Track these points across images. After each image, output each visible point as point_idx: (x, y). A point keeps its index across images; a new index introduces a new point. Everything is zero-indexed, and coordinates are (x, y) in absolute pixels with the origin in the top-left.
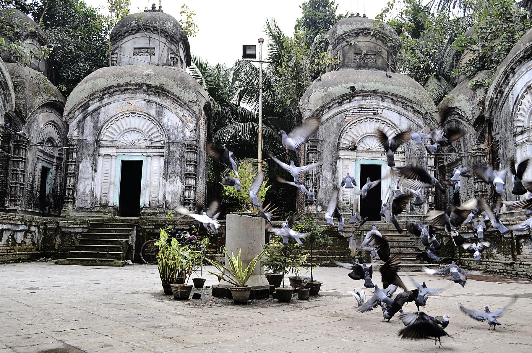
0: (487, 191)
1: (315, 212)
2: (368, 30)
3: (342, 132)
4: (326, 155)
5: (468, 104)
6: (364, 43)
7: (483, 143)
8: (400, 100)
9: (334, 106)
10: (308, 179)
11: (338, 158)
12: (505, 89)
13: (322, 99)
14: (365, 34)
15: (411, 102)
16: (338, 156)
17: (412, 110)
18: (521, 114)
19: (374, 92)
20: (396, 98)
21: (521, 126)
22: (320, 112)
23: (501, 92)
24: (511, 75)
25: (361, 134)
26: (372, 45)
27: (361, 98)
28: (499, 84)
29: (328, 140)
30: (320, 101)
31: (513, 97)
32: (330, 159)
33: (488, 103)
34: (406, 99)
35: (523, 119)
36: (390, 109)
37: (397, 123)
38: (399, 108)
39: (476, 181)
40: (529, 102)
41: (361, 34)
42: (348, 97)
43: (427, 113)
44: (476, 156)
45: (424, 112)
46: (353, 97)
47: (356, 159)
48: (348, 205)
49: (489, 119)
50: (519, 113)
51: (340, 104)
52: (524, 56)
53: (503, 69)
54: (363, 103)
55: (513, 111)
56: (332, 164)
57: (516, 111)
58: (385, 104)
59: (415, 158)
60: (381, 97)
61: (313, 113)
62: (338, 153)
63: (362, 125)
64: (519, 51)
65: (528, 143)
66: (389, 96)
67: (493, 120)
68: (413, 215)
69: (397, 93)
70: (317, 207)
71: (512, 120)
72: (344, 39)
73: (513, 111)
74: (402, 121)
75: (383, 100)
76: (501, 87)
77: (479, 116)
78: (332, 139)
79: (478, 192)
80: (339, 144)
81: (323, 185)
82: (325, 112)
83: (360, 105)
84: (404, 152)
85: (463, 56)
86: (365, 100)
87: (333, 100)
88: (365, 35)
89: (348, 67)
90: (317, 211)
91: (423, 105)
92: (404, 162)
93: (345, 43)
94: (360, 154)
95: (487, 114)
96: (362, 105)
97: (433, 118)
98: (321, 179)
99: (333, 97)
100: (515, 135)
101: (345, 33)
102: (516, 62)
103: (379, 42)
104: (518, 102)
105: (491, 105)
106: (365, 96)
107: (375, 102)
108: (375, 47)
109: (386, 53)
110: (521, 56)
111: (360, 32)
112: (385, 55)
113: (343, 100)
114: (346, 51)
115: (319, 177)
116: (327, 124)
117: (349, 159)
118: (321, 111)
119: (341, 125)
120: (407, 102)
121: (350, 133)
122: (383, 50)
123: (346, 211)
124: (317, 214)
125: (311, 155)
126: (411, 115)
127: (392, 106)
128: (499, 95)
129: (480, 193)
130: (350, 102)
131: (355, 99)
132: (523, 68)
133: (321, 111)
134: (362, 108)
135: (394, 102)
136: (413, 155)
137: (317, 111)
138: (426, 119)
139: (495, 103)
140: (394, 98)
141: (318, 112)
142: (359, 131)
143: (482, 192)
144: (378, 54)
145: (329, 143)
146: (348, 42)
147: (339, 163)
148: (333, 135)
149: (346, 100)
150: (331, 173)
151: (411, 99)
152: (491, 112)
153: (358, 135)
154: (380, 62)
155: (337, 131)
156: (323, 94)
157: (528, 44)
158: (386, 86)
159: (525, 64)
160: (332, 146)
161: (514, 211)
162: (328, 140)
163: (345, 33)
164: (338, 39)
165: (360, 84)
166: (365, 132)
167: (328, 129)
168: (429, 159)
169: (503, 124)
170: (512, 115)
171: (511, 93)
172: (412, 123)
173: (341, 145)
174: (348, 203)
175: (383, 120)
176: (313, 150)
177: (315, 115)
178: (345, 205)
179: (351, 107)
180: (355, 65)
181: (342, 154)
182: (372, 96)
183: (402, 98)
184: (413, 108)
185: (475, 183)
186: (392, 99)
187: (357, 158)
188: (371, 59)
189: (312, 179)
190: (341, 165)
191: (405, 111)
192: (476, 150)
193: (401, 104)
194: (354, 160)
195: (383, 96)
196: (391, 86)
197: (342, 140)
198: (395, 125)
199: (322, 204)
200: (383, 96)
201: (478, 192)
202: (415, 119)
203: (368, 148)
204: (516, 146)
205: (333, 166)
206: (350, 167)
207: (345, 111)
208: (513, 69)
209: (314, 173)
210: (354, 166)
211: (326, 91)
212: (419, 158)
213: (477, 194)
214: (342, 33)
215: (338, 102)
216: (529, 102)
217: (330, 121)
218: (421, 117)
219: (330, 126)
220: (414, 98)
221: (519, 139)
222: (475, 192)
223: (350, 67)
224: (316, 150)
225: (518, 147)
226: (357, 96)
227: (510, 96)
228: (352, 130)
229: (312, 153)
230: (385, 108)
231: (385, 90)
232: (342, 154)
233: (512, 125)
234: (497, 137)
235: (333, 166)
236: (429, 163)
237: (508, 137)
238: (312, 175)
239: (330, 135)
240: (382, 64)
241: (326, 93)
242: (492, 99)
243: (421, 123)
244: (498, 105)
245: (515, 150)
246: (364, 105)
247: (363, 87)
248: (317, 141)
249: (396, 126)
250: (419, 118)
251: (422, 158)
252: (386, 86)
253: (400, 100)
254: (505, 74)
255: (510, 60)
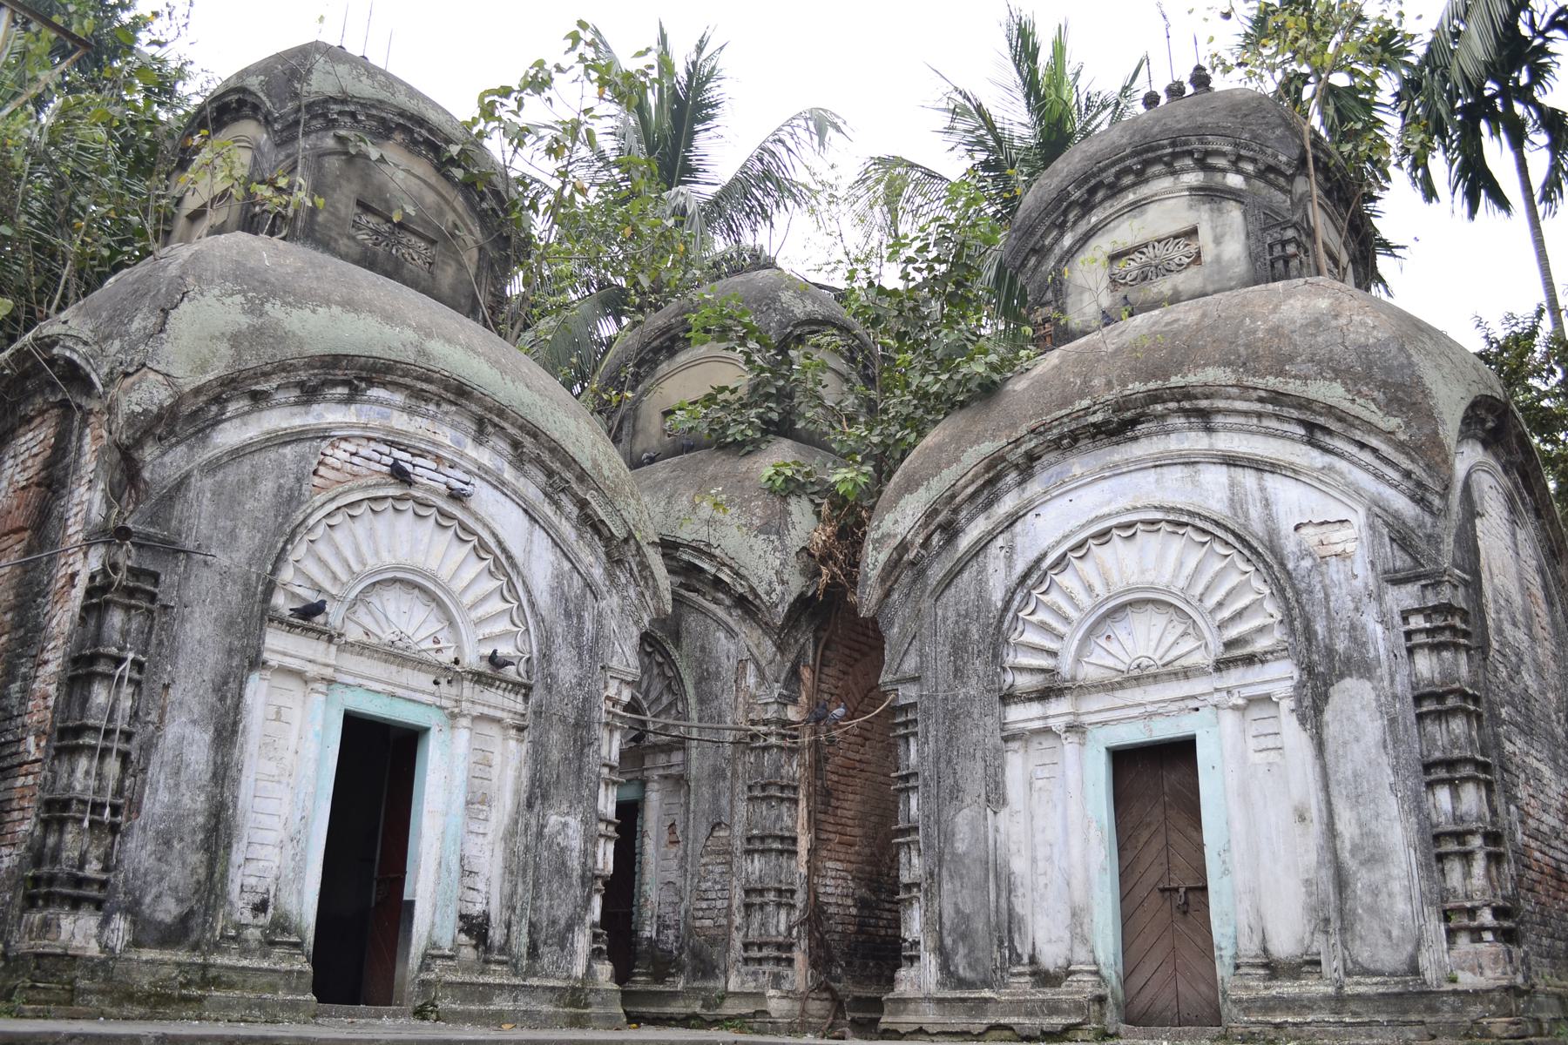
0: (793, 892)
1: (93, 949)
2: (430, 130)
3: (293, 534)
4: (200, 634)
5: (759, 543)
6: (402, 174)
7: (795, 702)
8: (546, 456)
9: (280, 396)
10: (76, 751)
11: (256, 662)
12: (971, 519)
13: (235, 339)
14: (415, 142)
15: (582, 477)
16: (259, 653)
17: (575, 511)
18: (1043, 627)
19: (459, 392)
20: (532, 447)
21: (1043, 671)
22: (209, 403)
23: (951, 531)
24: (1012, 477)
25: (372, 563)
26: (430, 198)
27: (399, 398)
28: (953, 497)
29: (223, 559)
30: (224, 349)
31: (1009, 559)
32: (213, 659)
33: (883, 557)
34: (569, 462)
35: (1052, 645)
36: (499, 485)
37: (516, 550)
38: (531, 490)
39: (758, 845)
40: (1090, 588)
41: (399, 137)
42: (351, 373)
43: (626, 541)
44: (766, 748)
45: (620, 533)
46: (371, 383)
47: (331, 682)
48: (264, 920)
49: (874, 620)
50: (1033, 618)
51: (309, 394)
52: (1106, 422)
53: (988, 448)
54: (400, 421)
55: (1006, 609)
56: (220, 688)
57: (1019, 610)
58: (484, 456)
59: (563, 719)
60: (481, 423)
61: (179, 400)
62: (261, 638)
63: (382, 524)
64: (1086, 403)
65: (1073, 738)
66: (511, 430)
67: (891, 623)
68: (534, 981)
69: (542, 423)
70: (105, 923)
71: (997, 642)
72: (331, 124)
73: (1006, 609)
74: (535, 548)
75: (480, 437)
76: (956, 511)
77: (802, 594)
78: (240, 556)
79: (761, 892)
80: (270, 588)
81: (157, 800)
82: (232, 408)
83: (391, 431)
84: (529, 688)
85: (664, 368)
86: (411, 411)
87: (283, 367)
88: (412, 145)
89: (325, 245)
90: (104, 947)
91: (620, 504)
92: (520, 729)
93: (330, 143)
94: (351, 662)
95: (867, 598)
96: (398, 433)
97: (644, 566)
98: (155, 759)
99: (289, 352)
100: (1008, 698)
101: (344, 102)
102: (1062, 437)
103: (459, 202)
104: (1033, 576)
105: (893, 567)
106: (418, 395)
107: (445, 432)
108: (440, 213)
109: (475, 253)
110: (1092, 419)
111: (399, 125)
112: (470, 258)
113: (324, 384)
114: (329, 179)
115: (148, 748)
116: (231, 475)
117: (298, 674)
118: (217, 400)
119: (290, 500)
120: (568, 475)
121: (323, 549)
122: (469, 239)
123: (245, 952)
124: (103, 967)
125: (116, 618)
126: (568, 530)
127: (509, 474)
128: (936, 538)
129: (771, 896)
130: (349, 400)
131: (375, 392)
132: (1078, 465)
133: (217, 400)
134: (392, 444)
135: (519, 459)
136: (556, 707)
137: (197, 391)
138: (619, 562)
139: (913, 564)
140: (528, 441)
141: (202, 398)
142: (364, 549)
143: (780, 892)
144: (440, 240)
145: (224, 574)
146: (341, 140)
147: (257, 689)
148: (248, 540)
149: (335, 384)
150: (207, 737)
151: (587, 465)
152: (888, 594)
153: (356, 568)
154: (447, 276)
155: (271, 525)
156: (244, 321)
157: (1136, 387)
158: (508, 378)
159: (1087, 451)
160: (234, 593)
161: (987, 993)
162: (223, 559)
163: (344, 102)
164: (309, 106)
165: (410, 335)
166: (388, 559)
167: (229, 500)
168: (605, 734)
169: (947, 649)
170: (1001, 621)
171: (1000, 541)
172: (567, 566)
173: (280, 601)
174: (260, 907)
175: (470, 522)
176: (131, 592)
177: (186, 410)
178: (247, 917)
179: (351, 426)
180: (356, 251)
181: (279, 644)
182: (445, 407)
183: (556, 449)
184: (583, 504)
185: (749, 852)
186: (516, 445)
187: (341, 677)
188: (415, 251)
189: (105, 752)
190: (261, 699)
191: (548, 509)
192: (766, 723)
193: (541, 478)
194: (322, 687)
195: (488, 419)
196: (521, 387)
197: (287, 574)
198: (509, 557)
199: (138, 902)
200: (488, 419)
201: (761, 892)
202: (582, 555)
203: (387, 636)
204: (1006, 740)
205: (222, 699)
206: (295, 715)
207: (323, 434)
208: (1032, 457)
209: (121, 724)
210: (319, 717)
211: (254, 309)
212: (577, 725)
213: (757, 900)
214: (330, 90)
215: (301, 385)
216: (1090, 588)
217: (246, 466)
218: (601, 551)
219: (241, 486)
220: (596, 465)
221: (1021, 715)
222: (748, 892)
223: (335, 253)
224: (152, 597)
225: (1014, 745)
226: (384, 385)
227: (994, 549)
228: (338, 536)
229: (128, 608)
230: (483, 473)
231: (502, 397)
232: (279, 644)
233: (996, 656)
234: (908, 694)
235: (222, 699)
236: (604, 751)
237: (969, 700)
238: (109, 733)
239: (233, 535)
240: (454, 289)
241: (257, 322)
242: (903, 547)
243: (598, 573)
244: (922, 573)
245: (999, 753)
246: (405, 434)
247: (422, 352)
248: (171, 549)
249: (514, 565)
250: (594, 552)
251: (588, 727)
252: (508, 378)
253: (546, 456)
254: (987, 470)
255: (1033, 423)
